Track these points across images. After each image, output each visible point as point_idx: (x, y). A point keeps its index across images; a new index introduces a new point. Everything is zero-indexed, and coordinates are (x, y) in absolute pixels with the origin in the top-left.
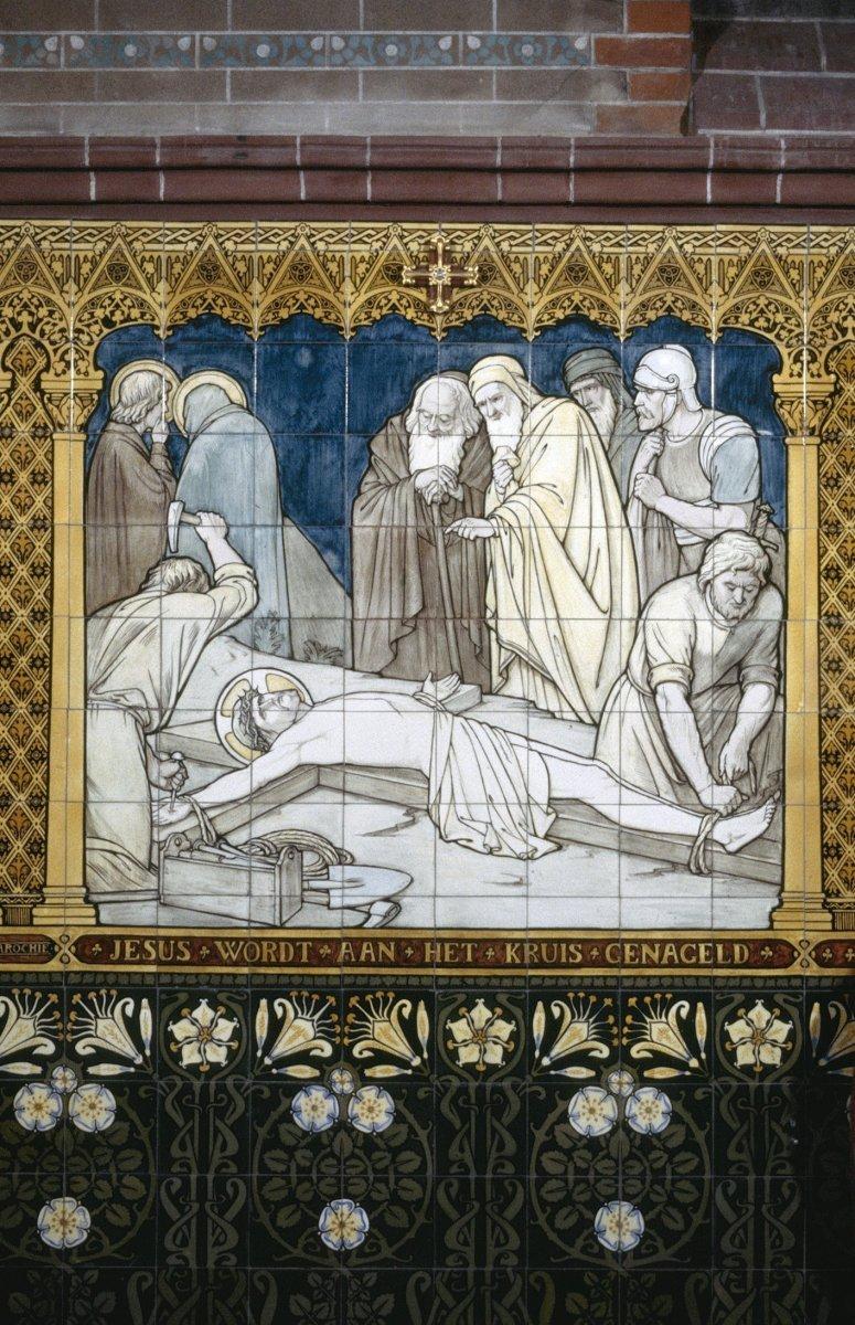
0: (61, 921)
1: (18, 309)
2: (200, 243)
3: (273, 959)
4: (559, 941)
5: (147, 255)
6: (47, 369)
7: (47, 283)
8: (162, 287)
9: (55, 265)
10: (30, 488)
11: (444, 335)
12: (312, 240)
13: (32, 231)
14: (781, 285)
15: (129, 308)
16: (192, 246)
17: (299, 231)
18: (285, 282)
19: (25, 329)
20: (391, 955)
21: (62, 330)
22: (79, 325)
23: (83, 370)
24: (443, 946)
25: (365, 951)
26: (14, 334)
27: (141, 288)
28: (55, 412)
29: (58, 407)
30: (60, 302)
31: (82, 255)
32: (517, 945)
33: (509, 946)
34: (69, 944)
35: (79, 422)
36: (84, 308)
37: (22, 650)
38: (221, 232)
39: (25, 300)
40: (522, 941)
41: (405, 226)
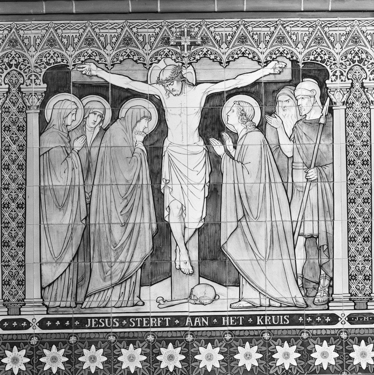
0: (341, 308)
1: (353, 55)
2: (161, 29)
3: (156, 325)
4: (280, 315)
5: (293, 32)
6: (328, 79)
7: (137, 45)
8: (338, 46)
9: (254, 36)
10: (360, 128)
11: (303, 65)
12: (284, 26)
13: (53, 25)
14: (364, 42)
15: (324, 55)
16: (157, 30)
17: (163, 23)
18: (236, 44)
19: (357, 63)
20: (207, 323)
21: (335, 64)
22: (341, 61)
23: (344, 80)
24: (229, 318)
25: (196, 321)
26: (352, 65)
27: (329, 47)
28: (370, 96)
29: (333, 95)
30: (333, 52)
31: (74, 35)
32: (262, 317)
33: (258, 317)
34: (345, 317)
35: (343, 101)
36: (306, 55)
37: (359, 195)
38: (246, 23)
39: (356, 51)
40: (264, 315)
41: (246, 20)
